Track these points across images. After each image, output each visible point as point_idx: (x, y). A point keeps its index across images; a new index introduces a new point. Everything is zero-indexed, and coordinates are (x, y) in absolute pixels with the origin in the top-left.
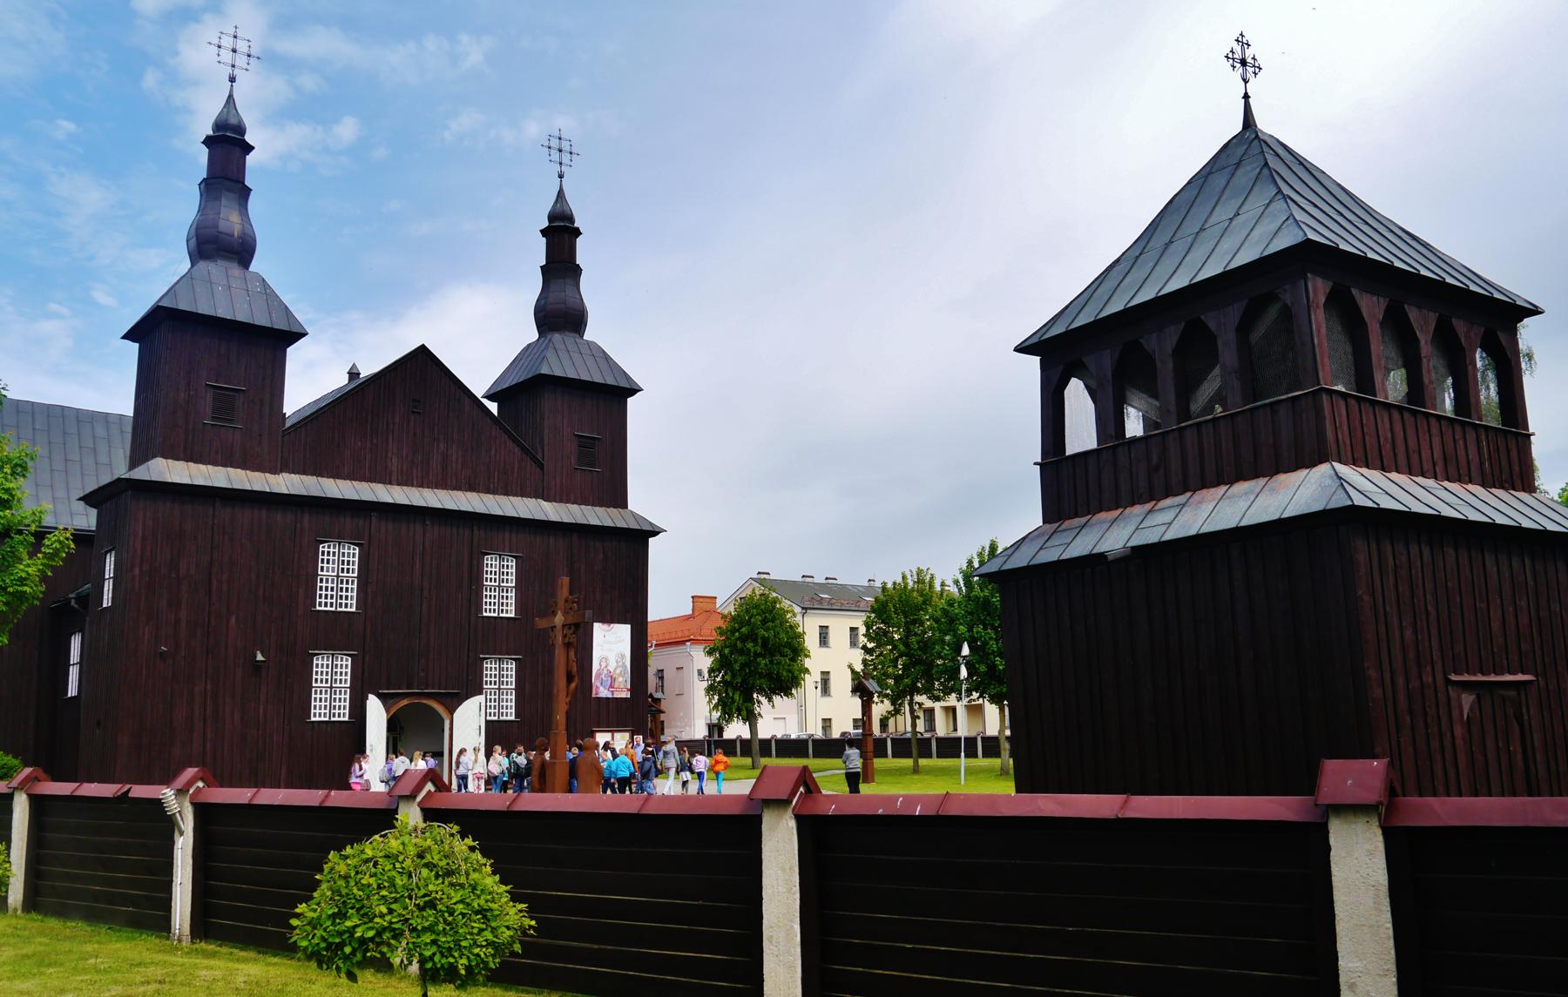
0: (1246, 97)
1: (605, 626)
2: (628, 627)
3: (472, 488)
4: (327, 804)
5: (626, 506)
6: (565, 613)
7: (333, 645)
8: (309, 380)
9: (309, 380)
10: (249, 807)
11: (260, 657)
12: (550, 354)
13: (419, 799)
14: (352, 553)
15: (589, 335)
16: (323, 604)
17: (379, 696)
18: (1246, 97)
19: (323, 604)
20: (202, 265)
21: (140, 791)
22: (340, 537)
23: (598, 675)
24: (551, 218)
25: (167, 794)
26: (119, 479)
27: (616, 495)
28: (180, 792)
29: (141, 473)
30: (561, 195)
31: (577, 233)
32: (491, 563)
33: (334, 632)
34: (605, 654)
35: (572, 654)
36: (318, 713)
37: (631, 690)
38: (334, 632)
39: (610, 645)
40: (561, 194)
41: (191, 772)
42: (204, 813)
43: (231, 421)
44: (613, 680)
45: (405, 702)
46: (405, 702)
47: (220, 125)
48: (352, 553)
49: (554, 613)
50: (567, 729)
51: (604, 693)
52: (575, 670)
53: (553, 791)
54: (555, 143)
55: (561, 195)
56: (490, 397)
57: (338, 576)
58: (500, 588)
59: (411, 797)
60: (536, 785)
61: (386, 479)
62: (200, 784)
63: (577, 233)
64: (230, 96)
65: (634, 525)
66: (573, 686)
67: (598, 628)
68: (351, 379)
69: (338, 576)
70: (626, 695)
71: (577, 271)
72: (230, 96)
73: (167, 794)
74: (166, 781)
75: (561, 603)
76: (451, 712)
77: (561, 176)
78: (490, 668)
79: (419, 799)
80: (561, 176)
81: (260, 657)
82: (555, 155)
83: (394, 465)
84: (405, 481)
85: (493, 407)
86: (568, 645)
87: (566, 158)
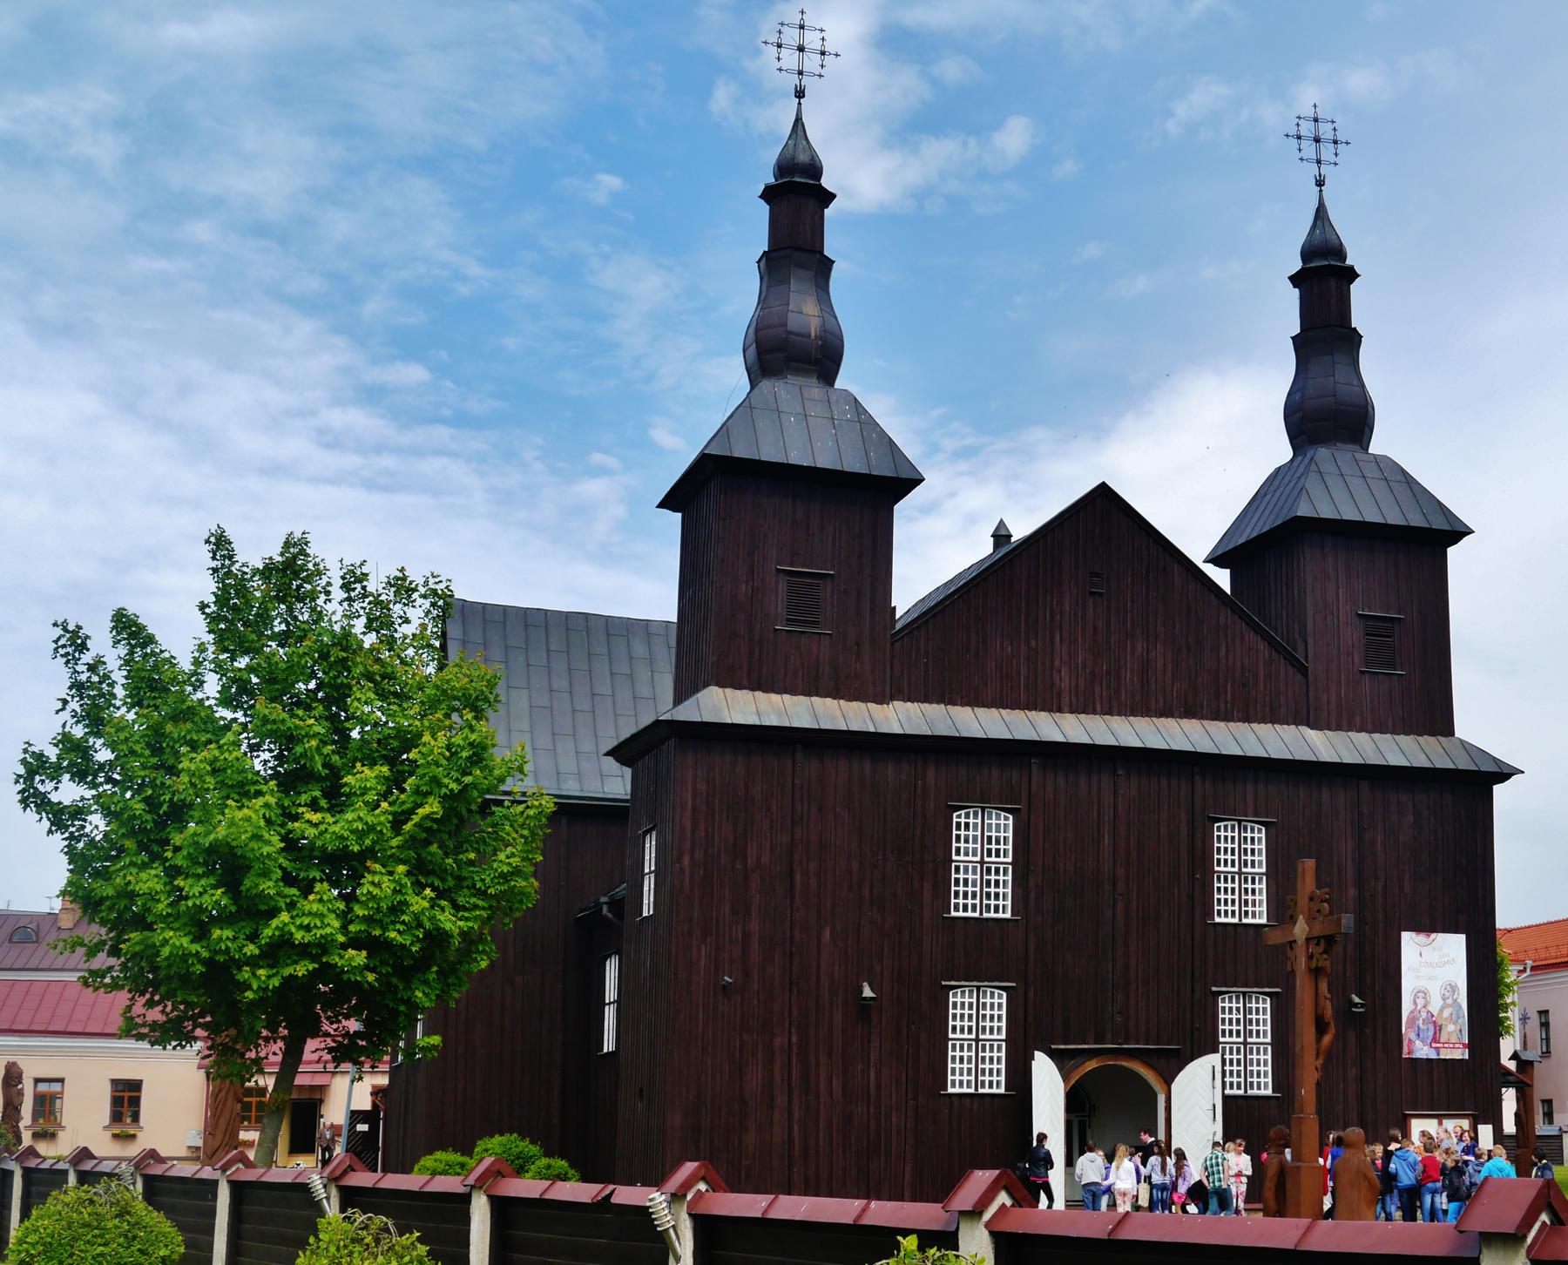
1: (1421, 938)
2: (1463, 937)
3: (1190, 711)
4: (866, 1221)
5: (1451, 733)
6: (1310, 920)
7: (978, 973)
8: (931, 554)
9: (931, 554)
10: (763, 1224)
11: (868, 992)
12: (1312, 484)
13: (987, 1216)
14: (1003, 825)
15: (1380, 444)
16: (963, 906)
17: (1053, 1055)
19: (963, 906)
20: (766, 385)
21: (626, 1195)
22: (984, 799)
23: (1412, 1020)
24: (1307, 254)
25: (656, 1199)
26: (657, 723)
27: (1435, 714)
28: (676, 1197)
29: (688, 712)
30: (1321, 214)
32: (1224, 835)
33: (977, 952)
34: (1422, 984)
35: (1323, 987)
36: (959, 1082)
37: (1470, 1046)
38: (977, 952)
39: (1432, 969)
41: (689, 1167)
42: (706, 1226)
43: (815, 624)
44: (1438, 1028)
45: (1092, 1065)
46: (1092, 1065)
47: (785, 167)
48: (1003, 825)
49: (1293, 920)
50: (1319, 1112)
51: (1422, 1051)
52: (1329, 1013)
53: (1298, 1216)
54: (1307, 129)
55: (1321, 214)
56: (1217, 559)
57: (982, 860)
58: (1241, 877)
59: (975, 1213)
60: (1272, 1205)
61: (1052, 704)
62: (702, 1187)
64: (798, 121)
65: (1464, 764)
66: (1327, 1039)
67: (1407, 938)
68: (996, 546)
69: (982, 860)
70: (1461, 1054)
71: (1354, 339)
72: (798, 121)
73: (656, 1199)
74: (657, 1181)
75: (1303, 901)
76: (1168, 1081)
77: (1320, 183)
78: (1229, 1008)
79: (987, 1216)
80: (1320, 183)
81: (868, 992)
82: (1309, 149)
83: (1064, 680)
84: (1083, 705)
85: (1222, 578)
86: (1316, 972)
87: (1327, 152)
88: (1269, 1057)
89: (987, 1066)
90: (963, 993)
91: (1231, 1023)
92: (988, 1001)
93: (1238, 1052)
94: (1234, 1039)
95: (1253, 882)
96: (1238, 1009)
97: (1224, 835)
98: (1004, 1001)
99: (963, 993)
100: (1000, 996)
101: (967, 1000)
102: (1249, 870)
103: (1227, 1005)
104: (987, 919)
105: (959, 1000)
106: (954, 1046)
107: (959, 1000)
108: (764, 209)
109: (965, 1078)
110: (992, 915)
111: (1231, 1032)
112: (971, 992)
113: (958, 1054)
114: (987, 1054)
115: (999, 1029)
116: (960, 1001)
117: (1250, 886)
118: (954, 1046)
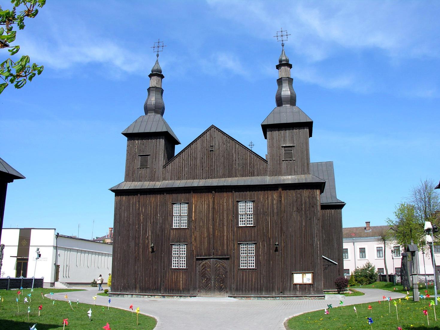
14: (185, 208)
64: (157, 61)
69: (180, 215)
72: (157, 61)
88: (254, 259)
89: (182, 262)
90: (176, 245)
91: (251, 251)
92: (182, 247)
93: (246, 258)
94: (245, 255)
95: (250, 216)
96: (246, 247)
97: (241, 205)
98: (186, 247)
99: (176, 245)
100: (185, 246)
101: (177, 247)
102: (249, 213)
103: (243, 246)
104: (181, 229)
105: (175, 247)
106: (174, 258)
107: (175, 247)
109: (176, 265)
110: (183, 227)
111: (251, 253)
112: (178, 245)
113: (175, 259)
114: (182, 259)
115: (185, 253)
116: (175, 248)
117: (249, 217)
118: (174, 258)
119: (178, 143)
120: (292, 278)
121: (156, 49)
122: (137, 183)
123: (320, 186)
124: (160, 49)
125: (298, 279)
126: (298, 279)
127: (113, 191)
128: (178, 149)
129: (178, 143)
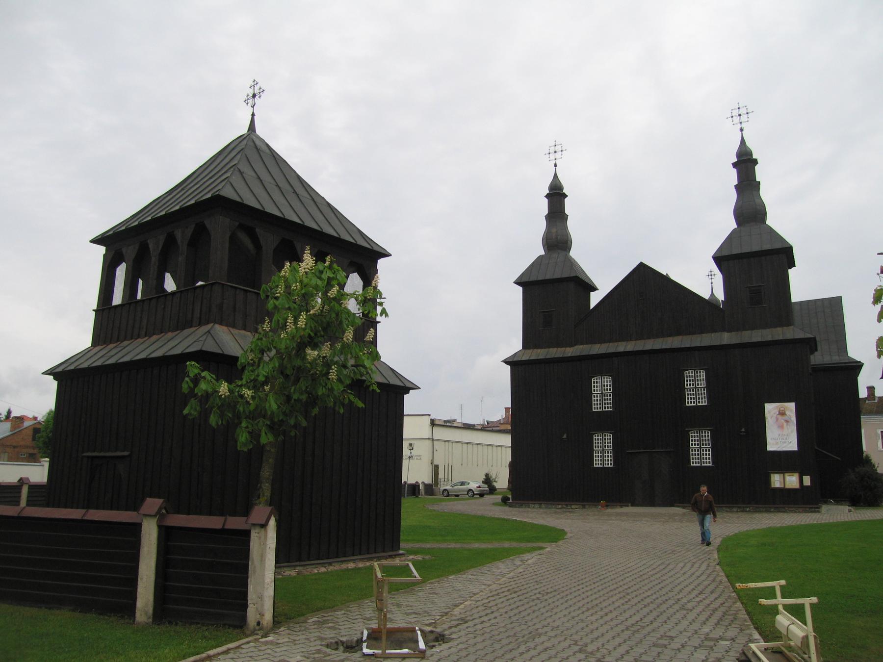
0: (253, 115)
7: (602, 429)
11: (565, 436)
14: (608, 381)
18: (253, 115)
19: (596, 407)
22: (601, 373)
31: (755, 162)
36: (597, 463)
38: (603, 422)
40: (743, 141)
48: (608, 381)
55: (743, 141)
57: (602, 392)
58: (696, 389)
63: (755, 162)
69: (602, 392)
77: (742, 130)
80: (742, 130)
81: (565, 436)
82: (737, 120)
84: (640, 337)
87: (744, 118)
108: (546, 200)
116: (597, 439)
119: (594, 289)
120: (768, 481)
121: (553, 156)
122: (539, 350)
123: (811, 344)
124: (558, 155)
125: (776, 481)
126: (776, 481)
127: (506, 362)
128: (595, 299)
129: (594, 289)
